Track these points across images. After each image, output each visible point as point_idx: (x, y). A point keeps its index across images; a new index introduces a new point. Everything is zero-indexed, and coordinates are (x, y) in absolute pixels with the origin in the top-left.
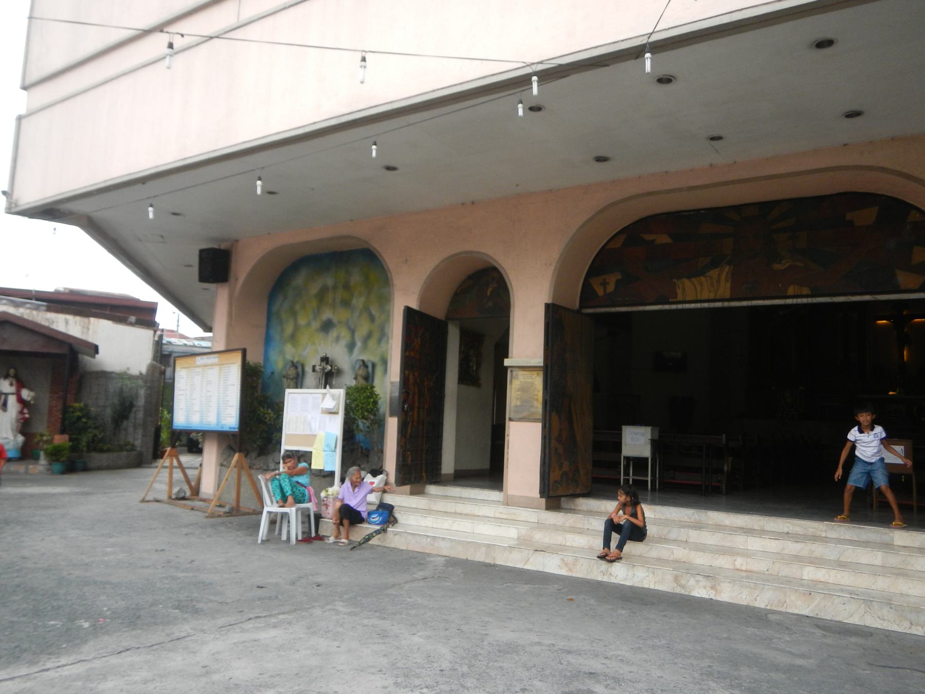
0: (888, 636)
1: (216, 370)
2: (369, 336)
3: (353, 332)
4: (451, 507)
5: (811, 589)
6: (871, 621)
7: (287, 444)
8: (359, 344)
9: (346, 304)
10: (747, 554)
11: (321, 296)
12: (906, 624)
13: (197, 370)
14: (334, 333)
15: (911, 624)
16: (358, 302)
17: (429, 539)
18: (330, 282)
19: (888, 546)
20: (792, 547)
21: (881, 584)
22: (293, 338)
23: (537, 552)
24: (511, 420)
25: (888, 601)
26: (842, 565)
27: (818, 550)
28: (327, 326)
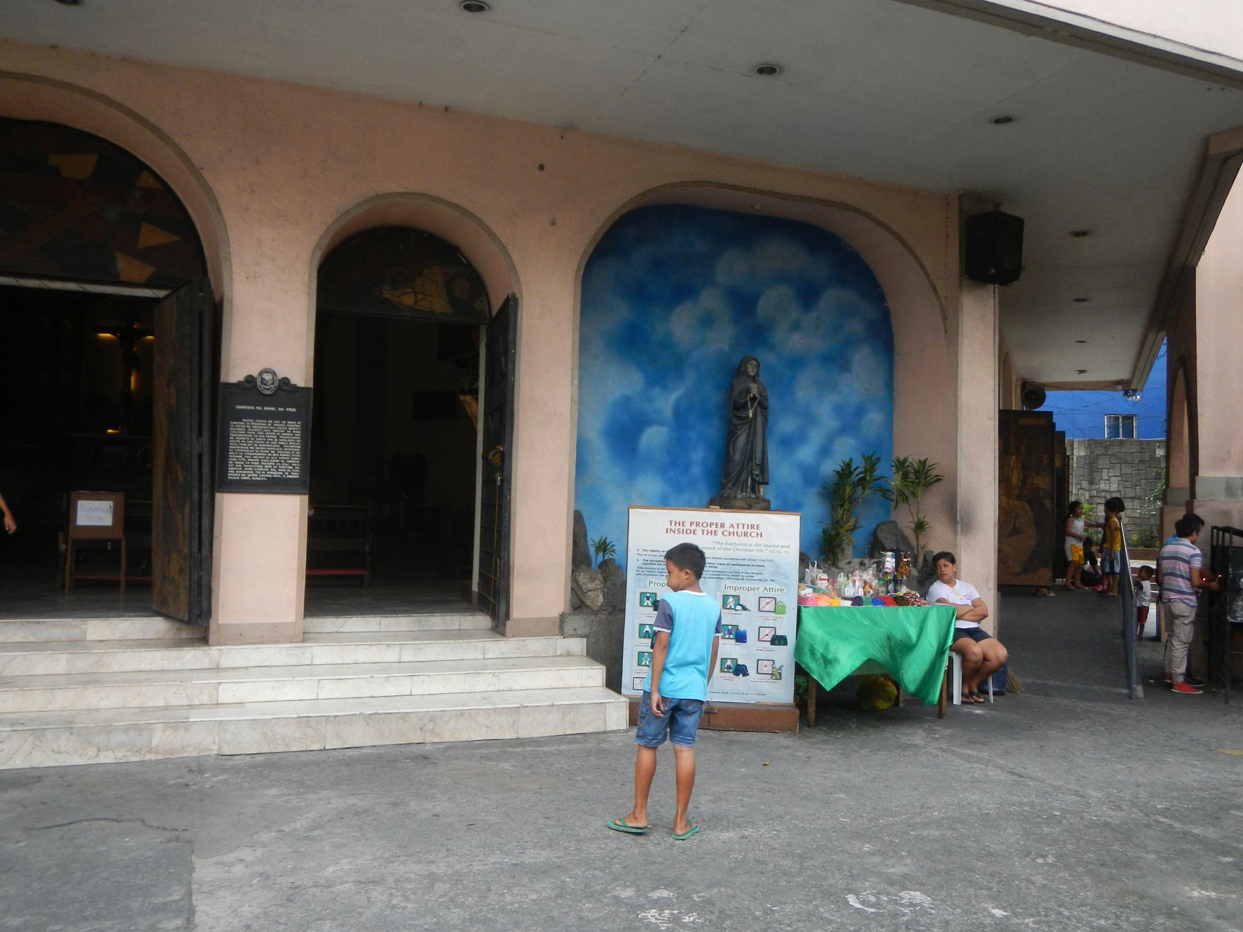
6: (42, 759)
12: (92, 752)
15: (99, 750)
25: (67, 725)
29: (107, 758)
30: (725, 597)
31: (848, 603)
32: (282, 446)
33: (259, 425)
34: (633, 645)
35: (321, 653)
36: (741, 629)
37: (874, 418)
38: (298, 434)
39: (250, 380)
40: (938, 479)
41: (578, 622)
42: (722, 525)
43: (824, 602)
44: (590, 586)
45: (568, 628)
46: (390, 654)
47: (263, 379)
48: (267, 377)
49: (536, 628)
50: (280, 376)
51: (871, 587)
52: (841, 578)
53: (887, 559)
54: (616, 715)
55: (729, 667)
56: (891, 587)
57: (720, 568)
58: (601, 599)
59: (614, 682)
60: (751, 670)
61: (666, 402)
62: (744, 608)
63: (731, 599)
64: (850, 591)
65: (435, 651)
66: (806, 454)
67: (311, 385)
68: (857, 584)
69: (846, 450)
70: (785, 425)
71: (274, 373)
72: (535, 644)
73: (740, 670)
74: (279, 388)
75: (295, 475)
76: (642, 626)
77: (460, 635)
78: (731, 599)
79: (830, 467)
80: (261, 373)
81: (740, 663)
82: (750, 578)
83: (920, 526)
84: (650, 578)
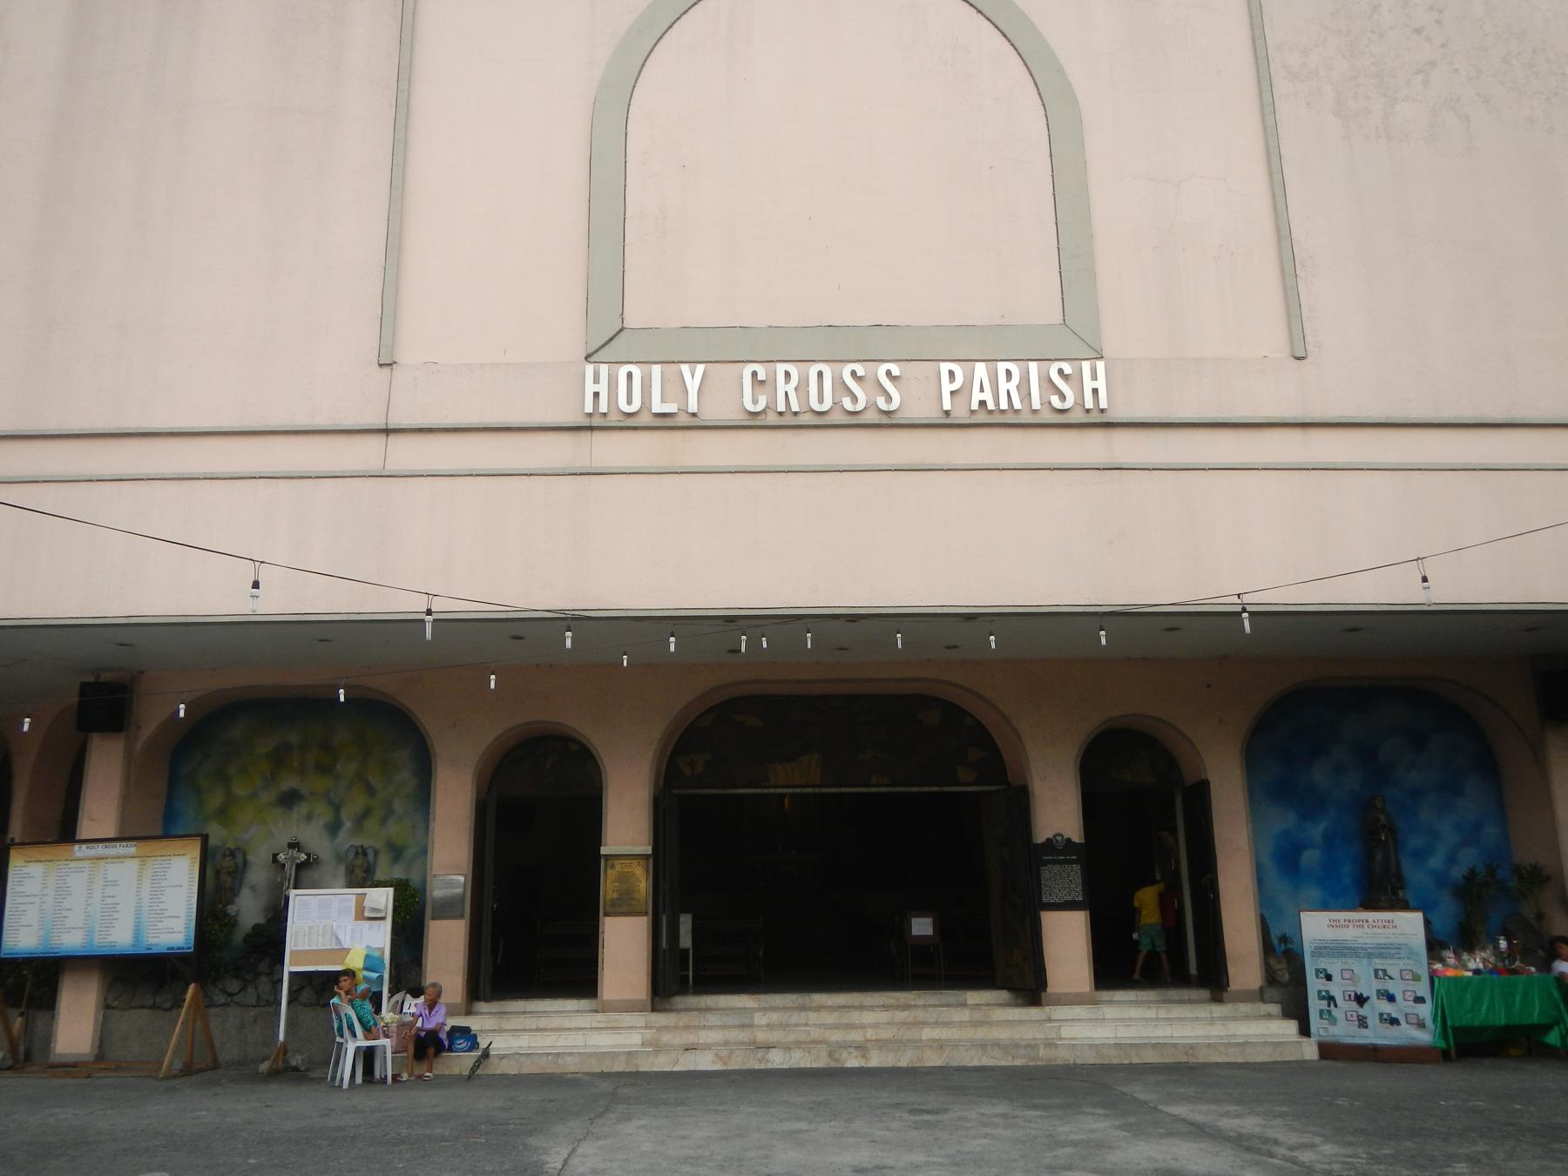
0: (1003, 1068)
1: (134, 865)
2: (366, 814)
3: (337, 809)
4: (531, 1022)
5: (940, 1045)
6: (986, 1061)
7: (291, 964)
8: (348, 824)
9: (324, 769)
10: (862, 1027)
11: (279, 759)
12: (1010, 1058)
13: (73, 864)
14: (302, 809)
15: (1013, 1057)
16: (347, 768)
17: (550, 1057)
18: (294, 738)
19: (964, 1005)
20: (901, 1016)
21: (981, 1033)
22: (223, 814)
23: (687, 1052)
24: (606, 915)
25: (997, 1044)
26: (937, 1024)
27: (921, 1015)
28: (289, 800)
29: (1018, 1063)
30: (1376, 971)
31: (1470, 974)
32: (1071, 881)
33: (1057, 868)
34: (1315, 1006)
35: (1109, 1012)
36: (1391, 992)
37: (1491, 832)
38: (1079, 872)
39: (1049, 840)
40: (1548, 878)
41: (1272, 992)
42: (1367, 921)
43: (1451, 973)
44: (1279, 967)
45: (1267, 996)
46: (1151, 1013)
48: (1059, 838)
49: (1245, 997)
50: (1066, 837)
51: (1489, 962)
52: (1465, 956)
53: (1501, 942)
54: (1310, 1051)
55: (1386, 1020)
56: (1507, 962)
57: (1369, 950)
58: (1287, 976)
59: (1305, 1030)
60: (1403, 1021)
61: (1316, 831)
62: (1391, 978)
63: (1380, 972)
64: (1472, 965)
65: (1178, 1011)
66: (1436, 862)
67: (1083, 841)
68: (1478, 960)
69: (1469, 858)
70: (1415, 841)
71: (1062, 836)
72: (1245, 1008)
73: (1394, 1022)
74: (1066, 844)
75: (1080, 898)
76: (1320, 992)
77: (1190, 1002)
78: (1380, 972)
79: (1457, 873)
80: (1055, 836)
81: (1394, 1016)
82: (1392, 957)
83: (1540, 916)
84: (1321, 959)
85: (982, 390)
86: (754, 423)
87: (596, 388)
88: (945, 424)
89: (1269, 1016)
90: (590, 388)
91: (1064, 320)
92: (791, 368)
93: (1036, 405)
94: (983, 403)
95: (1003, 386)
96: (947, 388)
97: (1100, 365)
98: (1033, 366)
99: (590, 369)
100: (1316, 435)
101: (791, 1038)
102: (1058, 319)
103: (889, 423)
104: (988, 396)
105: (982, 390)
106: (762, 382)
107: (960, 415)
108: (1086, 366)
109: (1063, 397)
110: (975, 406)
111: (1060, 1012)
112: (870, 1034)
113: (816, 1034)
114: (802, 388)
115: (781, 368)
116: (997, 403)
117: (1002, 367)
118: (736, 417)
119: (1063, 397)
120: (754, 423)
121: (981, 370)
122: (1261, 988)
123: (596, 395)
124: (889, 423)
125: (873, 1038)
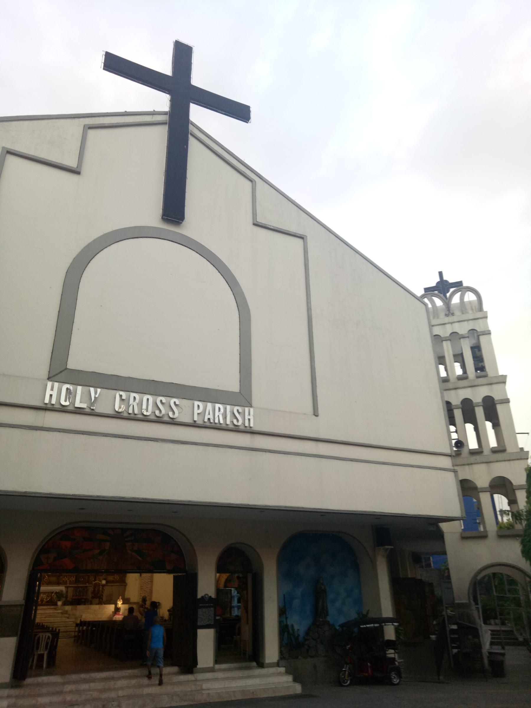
33: (204, 610)
39: (202, 597)
41: (282, 663)
45: (280, 665)
47: (206, 597)
48: (207, 596)
49: (271, 665)
61: (299, 592)
71: (208, 595)
72: (272, 670)
80: (205, 595)
85: (209, 414)
86: (118, 416)
87: (51, 393)
88: (194, 425)
89: (280, 674)
90: (48, 392)
91: (240, 391)
92: (137, 396)
93: (228, 422)
94: (209, 419)
95: (217, 413)
96: (196, 411)
97: (252, 410)
98: (228, 407)
99: (49, 384)
100: (321, 445)
101: (83, 697)
102: (239, 391)
103: (173, 422)
104: (211, 417)
105: (209, 414)
106: (123, 400)
107: (200, 422)
108: (247, 409)
109: (238, 421)
110: (206, 420)
111: (200, 676)
112: (121, 693)
113: (95, 694)
114: (140, 404)
115: (133, 395)
116: (214, 420)
117: (217, 406)
118: (111, 412)
119: (238, 421)
120: (118, 416)
121: (209, 405)
122: (278, 661)
123: (51, 396)
124: (173, 422)
125: (121, 695)
